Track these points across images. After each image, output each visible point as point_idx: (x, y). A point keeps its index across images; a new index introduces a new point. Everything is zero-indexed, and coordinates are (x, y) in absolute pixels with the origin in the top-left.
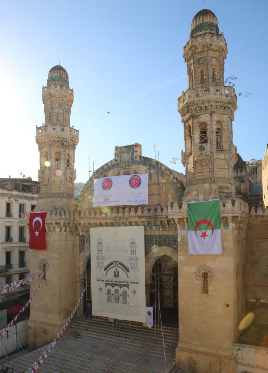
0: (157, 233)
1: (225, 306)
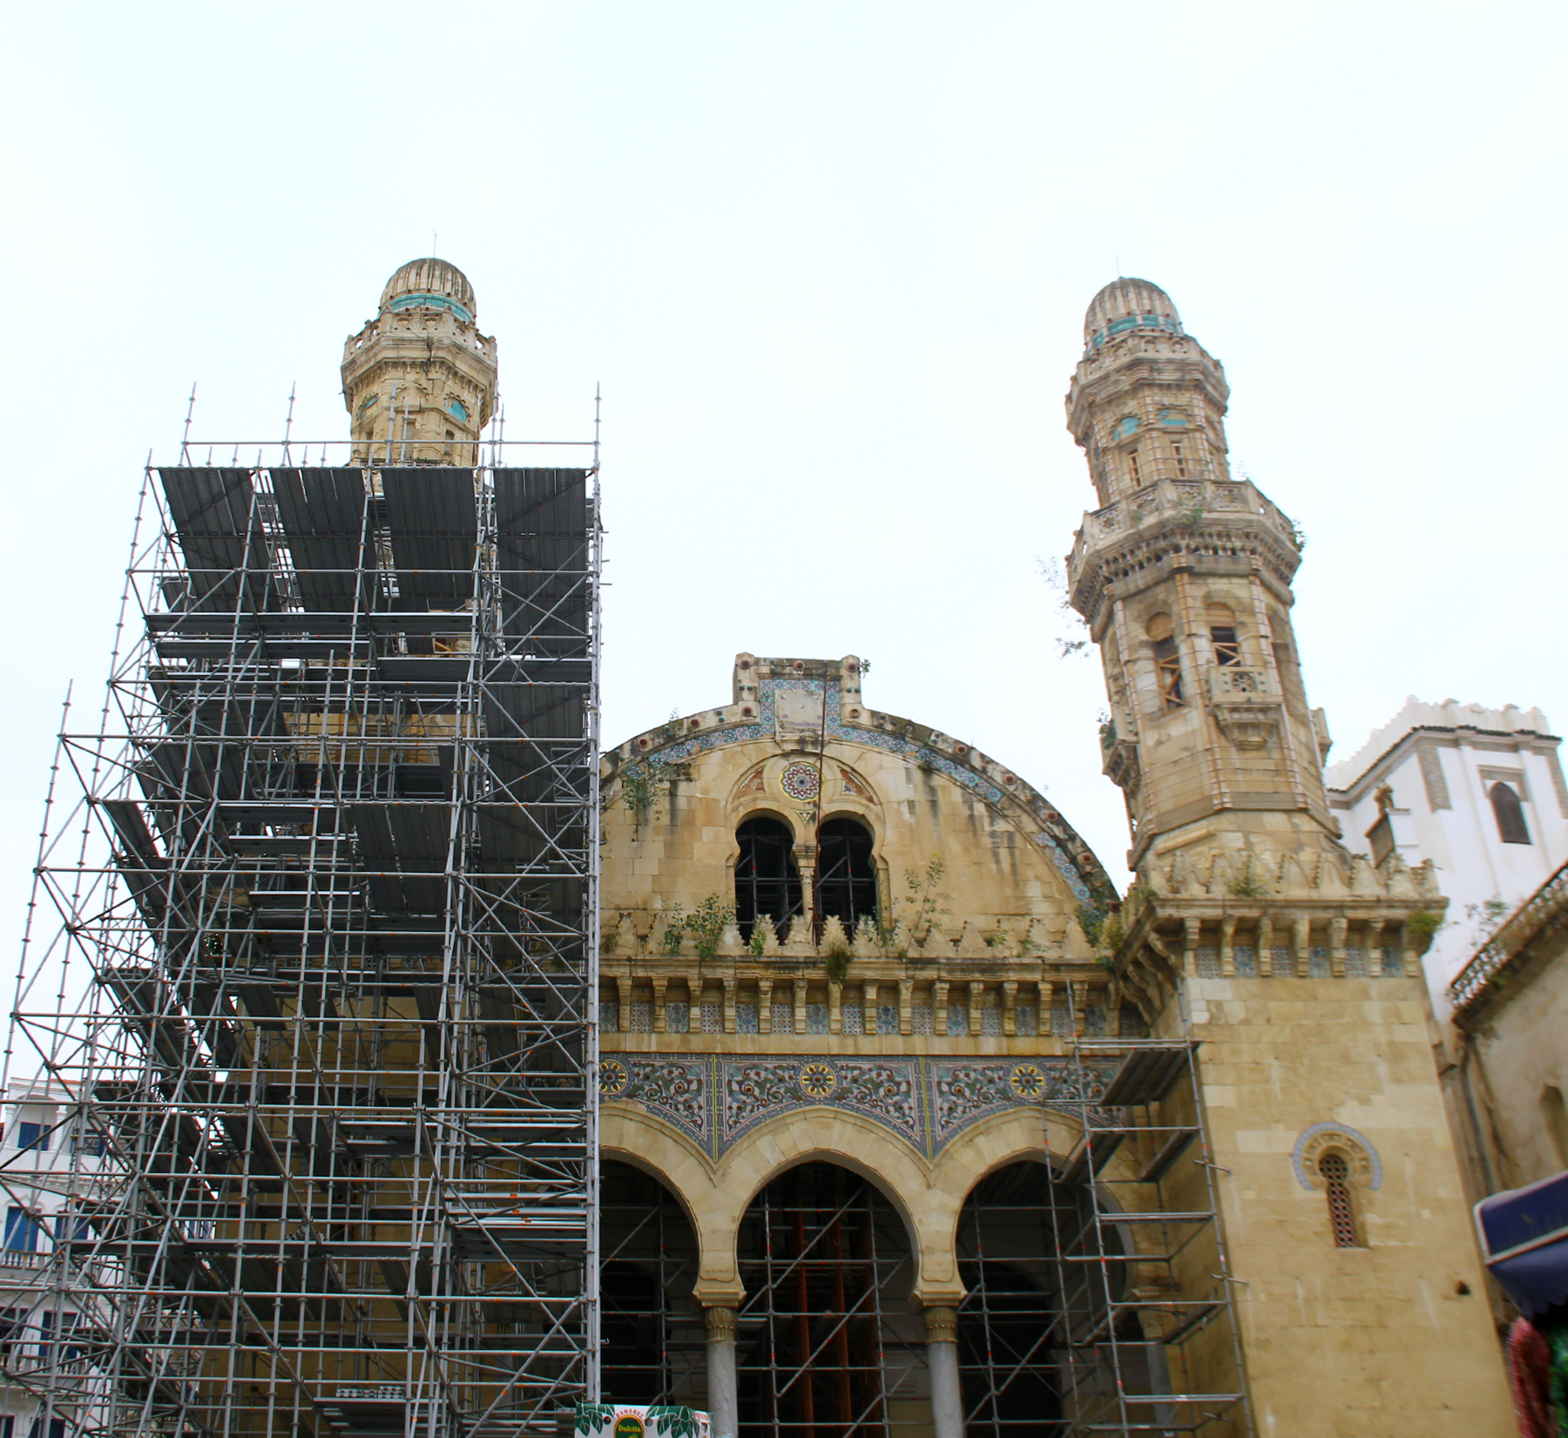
0: (989, 1045)
1: (1453, 1293)
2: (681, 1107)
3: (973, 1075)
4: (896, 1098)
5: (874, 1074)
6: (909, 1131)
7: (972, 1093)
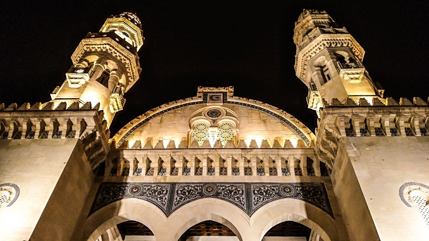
2: (159, 199)
3: (266, 188)
4: (237, 196)
5: (230, 188)
6: (242, 206)
7: (266, 194)
